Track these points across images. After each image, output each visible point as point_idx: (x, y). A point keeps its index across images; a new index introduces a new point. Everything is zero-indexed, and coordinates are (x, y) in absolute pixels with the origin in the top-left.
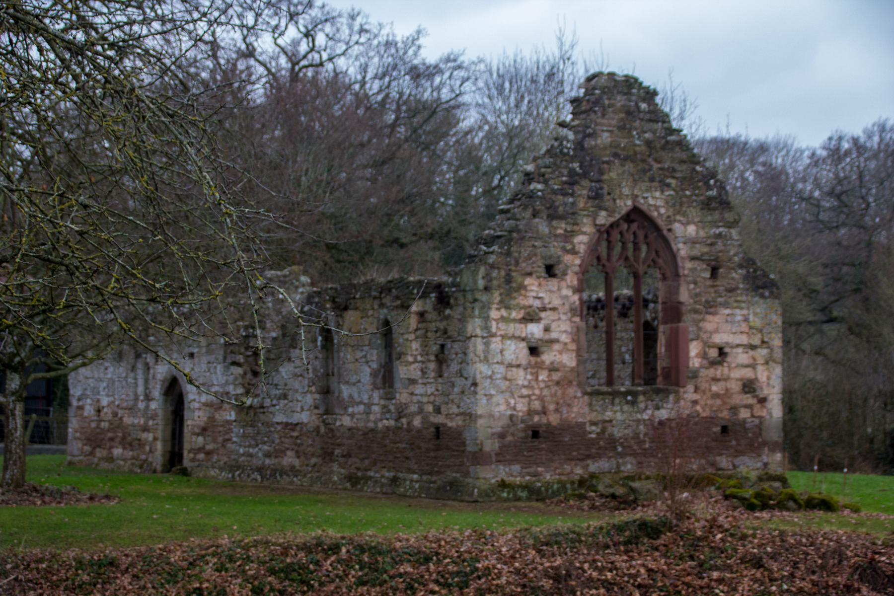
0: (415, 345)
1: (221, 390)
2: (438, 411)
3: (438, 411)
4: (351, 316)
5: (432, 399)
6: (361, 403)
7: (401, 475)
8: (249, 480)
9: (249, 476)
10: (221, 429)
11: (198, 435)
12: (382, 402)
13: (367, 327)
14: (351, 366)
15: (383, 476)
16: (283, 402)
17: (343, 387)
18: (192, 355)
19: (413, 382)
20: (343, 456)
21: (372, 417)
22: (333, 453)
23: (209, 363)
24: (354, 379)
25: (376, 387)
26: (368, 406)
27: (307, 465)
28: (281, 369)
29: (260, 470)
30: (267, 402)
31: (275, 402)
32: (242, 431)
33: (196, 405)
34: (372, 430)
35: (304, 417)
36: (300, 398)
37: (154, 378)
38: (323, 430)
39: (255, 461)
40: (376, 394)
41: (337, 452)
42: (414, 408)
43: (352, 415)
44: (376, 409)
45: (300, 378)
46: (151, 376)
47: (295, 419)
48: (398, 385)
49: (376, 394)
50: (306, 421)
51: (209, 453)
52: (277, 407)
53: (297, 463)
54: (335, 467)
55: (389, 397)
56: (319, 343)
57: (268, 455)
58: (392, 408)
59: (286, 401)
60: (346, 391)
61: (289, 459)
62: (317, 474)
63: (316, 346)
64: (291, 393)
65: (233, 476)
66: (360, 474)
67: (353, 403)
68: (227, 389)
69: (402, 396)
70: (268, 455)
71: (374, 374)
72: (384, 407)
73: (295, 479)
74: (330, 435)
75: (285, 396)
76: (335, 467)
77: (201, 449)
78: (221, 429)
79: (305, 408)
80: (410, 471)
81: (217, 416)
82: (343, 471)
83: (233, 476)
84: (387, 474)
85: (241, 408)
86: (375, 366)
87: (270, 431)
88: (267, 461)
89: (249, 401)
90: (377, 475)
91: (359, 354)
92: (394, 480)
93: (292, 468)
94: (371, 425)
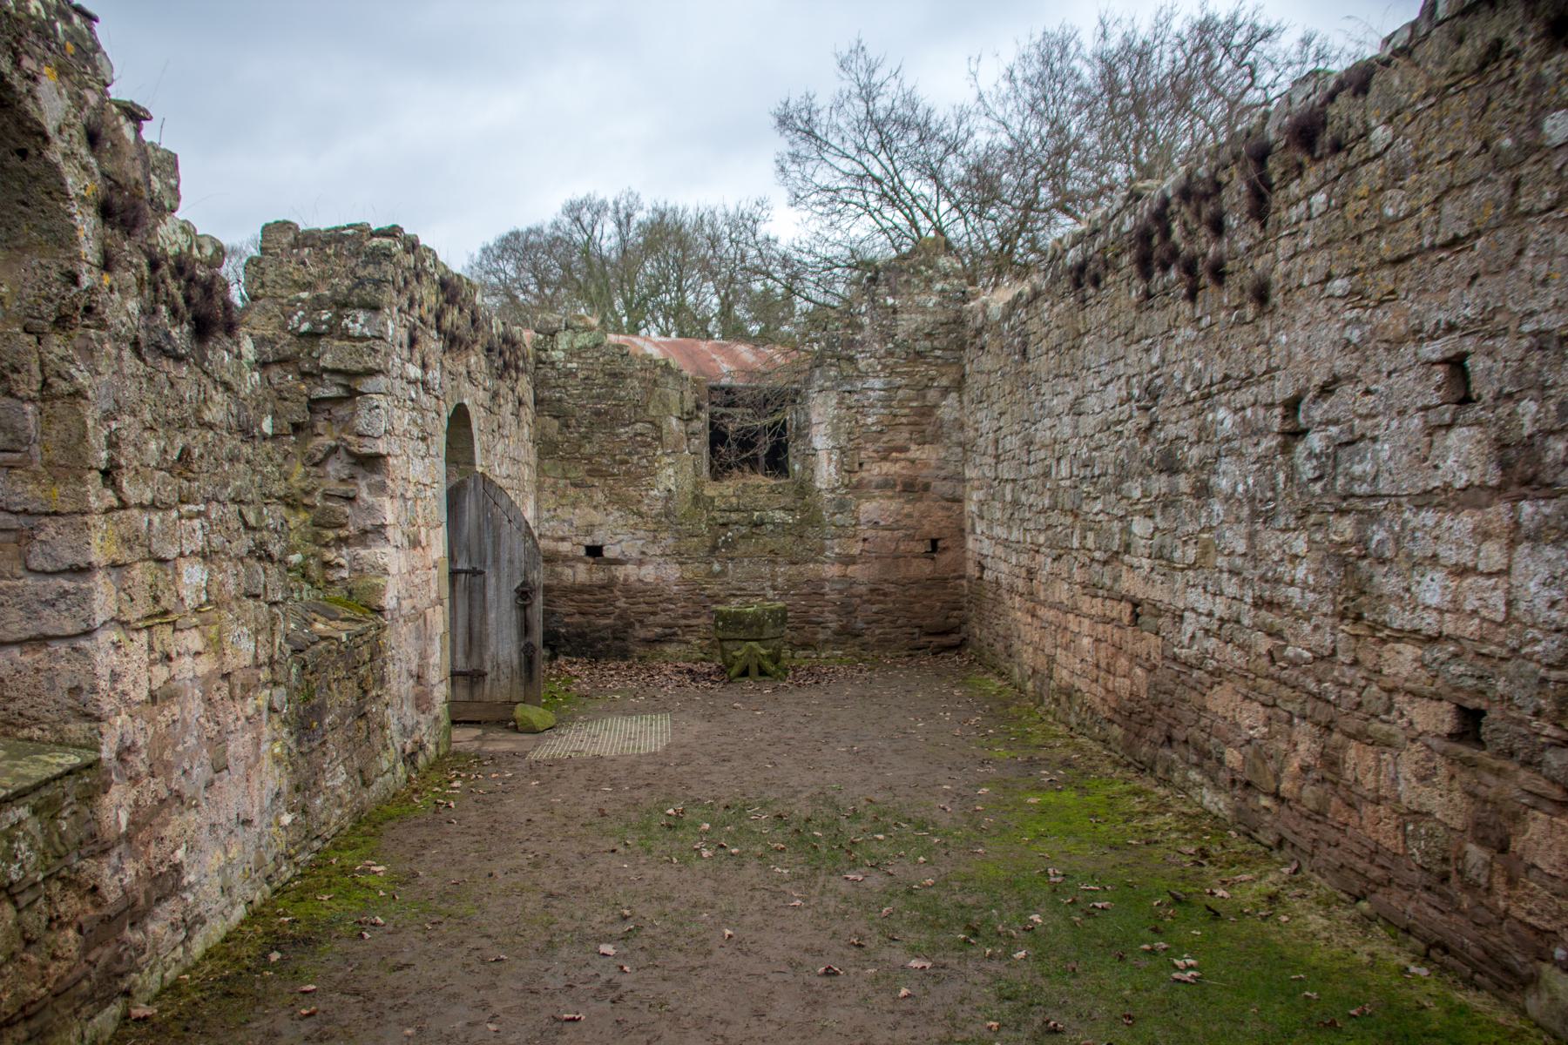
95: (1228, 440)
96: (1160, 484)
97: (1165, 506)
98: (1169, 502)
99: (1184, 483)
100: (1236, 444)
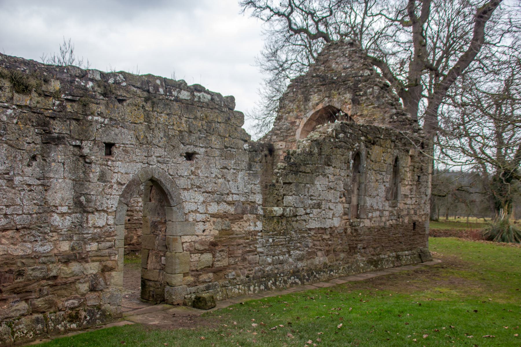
0: (409, 175)
1: (243, 199)
2: (415, 214)
3: (415, 214)
4: (376, 150)
5: (414, 206)
6: (378, 210)
7: (400, 253)
8: (288, 286)
9: (285, 282)
10: (241, 241)
11: (202, 252)
12: (390, 209)
13: (387, 159)
14: (372, 184)
15: (389, 256)
16: (315, 211)
17: (367, 199)
18: (189, 156)
19: (406, 196)
20: (364, 248)
21: (384, 219)
22: (356, 247)
23: (225, 168)
24: (375, 193)
25: (387, 199)
26: (382, 211)
27: (337, 260)
28: (316, 182)
29: (296, 273)
30: (301, 211)
31: (308, 211)
32: (271, 240)
33: (199, 217)
34: (383, 228)
35: (336, 222)
36: (332, 207)
37: (102, 178)
38: (349, 231)
39: (286, 267)
40: (387, 204)
41: (359, 246)
42: (405, 212)
43: (371, 219)
44: (387, 213)
45: (333, 191)
46: (94, 176)
47: (328, 224)
48: (399, 198)
49: (387, 204)
50: (337, 225)
51: (217, 271)
52: (311, 215)
53: (325, 259)
54: (358, 257)
55: (394, 206)
56: (351, 165)
57: (300, 259)
58: (395, 212)
59: (319, 210)
60: (369, 202)
61: (320, 259)
62: (347, 265)
63: (348, 168)
64: (323, 202)
65: (266, 287)
66: (375, 258)
67: (372, 209)
68: (251, 198)
69: (401, 205)
70: (300, 259)
71: (387, 191)
72: (391, 212)
73: (332, 273)
74: (355, 234)
75: (319, 206)
76: (358, 257)
77: (209, 268)
78: (241, 241)
79: (337, 215)
80: (403, 250)
81: (235, 228)
82: (364, 258)
83: (266, 287)
84: (391, 255)
85: (268, 218)
86: (388, 185)
87: (304, 237)
88: (300, 265)
89: (278, 210)
90: (386, 256)
91: (379, 177)
92: (398, 257)
93: (325, 264)
94: (382, 224)
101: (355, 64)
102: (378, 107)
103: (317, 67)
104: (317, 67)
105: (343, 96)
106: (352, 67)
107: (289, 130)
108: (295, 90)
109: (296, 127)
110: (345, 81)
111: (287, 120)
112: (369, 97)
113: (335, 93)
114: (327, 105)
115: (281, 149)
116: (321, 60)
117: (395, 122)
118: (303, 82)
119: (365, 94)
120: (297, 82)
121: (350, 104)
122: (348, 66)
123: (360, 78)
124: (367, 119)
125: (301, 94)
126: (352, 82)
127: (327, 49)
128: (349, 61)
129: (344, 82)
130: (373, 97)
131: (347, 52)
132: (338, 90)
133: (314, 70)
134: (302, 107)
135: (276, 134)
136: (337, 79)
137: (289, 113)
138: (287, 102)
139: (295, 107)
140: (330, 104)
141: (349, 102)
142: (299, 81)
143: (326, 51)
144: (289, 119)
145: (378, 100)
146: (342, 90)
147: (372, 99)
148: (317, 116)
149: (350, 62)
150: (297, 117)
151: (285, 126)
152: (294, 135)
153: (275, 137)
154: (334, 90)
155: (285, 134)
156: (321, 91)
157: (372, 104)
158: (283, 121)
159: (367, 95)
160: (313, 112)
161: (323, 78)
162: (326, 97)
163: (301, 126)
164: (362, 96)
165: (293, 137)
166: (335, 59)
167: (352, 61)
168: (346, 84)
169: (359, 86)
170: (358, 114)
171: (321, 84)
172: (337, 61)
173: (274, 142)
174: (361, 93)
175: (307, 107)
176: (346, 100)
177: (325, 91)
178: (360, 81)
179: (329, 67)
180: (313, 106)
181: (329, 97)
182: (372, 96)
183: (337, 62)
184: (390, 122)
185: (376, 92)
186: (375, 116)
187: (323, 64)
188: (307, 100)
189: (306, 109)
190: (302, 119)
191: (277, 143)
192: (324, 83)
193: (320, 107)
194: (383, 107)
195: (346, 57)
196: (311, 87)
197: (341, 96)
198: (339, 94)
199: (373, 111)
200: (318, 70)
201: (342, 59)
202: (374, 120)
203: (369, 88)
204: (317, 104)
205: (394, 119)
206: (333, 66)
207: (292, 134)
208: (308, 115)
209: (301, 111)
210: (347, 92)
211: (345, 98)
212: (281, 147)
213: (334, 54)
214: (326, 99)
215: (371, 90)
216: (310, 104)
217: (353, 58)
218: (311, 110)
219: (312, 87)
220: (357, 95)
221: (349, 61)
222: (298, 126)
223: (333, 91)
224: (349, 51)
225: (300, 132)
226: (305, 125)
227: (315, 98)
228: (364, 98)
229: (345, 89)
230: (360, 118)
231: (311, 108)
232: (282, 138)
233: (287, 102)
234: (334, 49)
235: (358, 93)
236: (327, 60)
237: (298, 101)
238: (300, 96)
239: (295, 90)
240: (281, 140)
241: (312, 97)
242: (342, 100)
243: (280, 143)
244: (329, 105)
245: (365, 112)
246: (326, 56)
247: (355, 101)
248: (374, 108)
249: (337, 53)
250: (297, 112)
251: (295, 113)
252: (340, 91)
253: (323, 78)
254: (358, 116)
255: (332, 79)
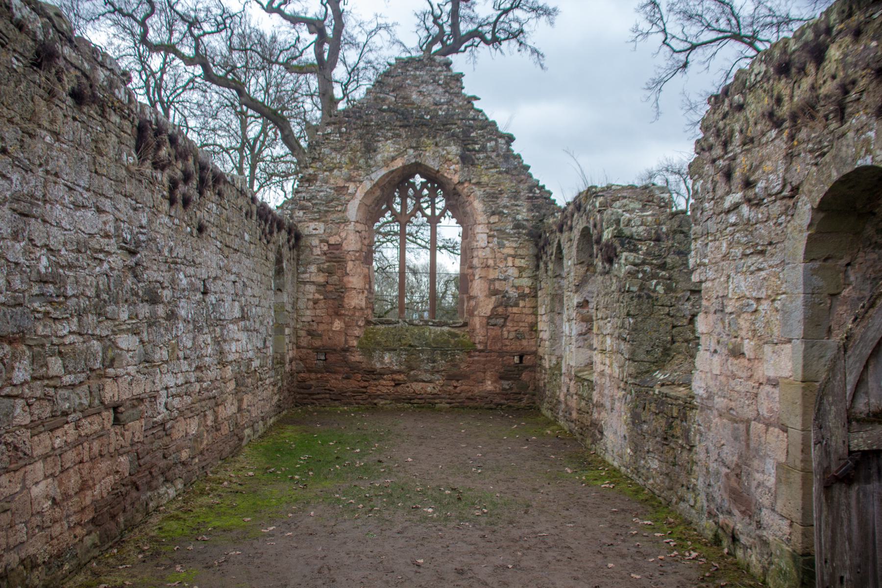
95: (184, 290)
96: (144, 310)
97: (150, 326)
98: (152, 323)
99: (161, 310)
100: (186, 293)
101: (456, 100)
102: (507, 172)
103: (382, 96)
104: (382, 96)
105: (443, 150)
106: (449, 103)
107: (332, 201)
108: (344, 130)
109: (347, 198)
110: (446, 123)
111: (327, 183)
112: (489, 154)
113: (428, 142)
114: (413, 161)
115: (315, 235)
116: (389, 85)
117: (537, 198)
118: (361, 117)
119: (483, 149)
120: (348, 116)
121: (457, 163)
122: (442, 101)
123: (471, 122)
124: (488, 189)
125: (357, 139)
126: (459, 128)
127: (402, 68)
128: (446, 92)
129: (444, 125)
130: (498, 155)
131: (442, 77)
132: (434, 137)
133: (375, 99)
134: (362, 161)
135: (302, 208)
136: (431, 118)
137: (331, 170)
138: (326, 150)
139: (345, 159)
140: (419, 160)
141: (454, 160)
142: (351, 115)
143: (399, 71)
144: (332, 181)
145: (506, 161)
146: (441, 139)
147: (496, 159)
148: (387, 180)
149: (447, 94)
150: (350, 179)
151: (322, 194)
152: (345, 210)
153: (301, 213)
154: (428, 137)
155: (323, 208)
156: (399, 136)
157: (495, 167)
158: (318, 183)
159: (486, 152)
160: (384, 171)
161: (403, 114)
162: (411, 147)
163: (360, 195)
164: (479, 152)
165: (341, 215)
166: (418, 87)
167: (450, 94)
168: (449, 130)
169: (472, 135)
170: (473, 181)
171: (401, 124)
172: (421, 88)
173: (300, 222)
174: (477, 147)
175: (372, 162)
176: (450, 157)
177: (407, 137)
178: (472, 127)
179: (404, 98)
180: (384, 161)
181: (415, 149)
182: (495, 154)
183: (420, 92)
184: (529, 198)
185: (502, 148)
186: (502, 187)
187: (393, 91)
188: (370, 149)
189: (370, 166)
190: (361, 182)
191: (306, 224)
192: (406, 122)
193: (399, 163)
194: (514, 172)
195: (439, 85)
196: (380, 127)
197: (440, 149)
198: (436, 145)
199: (498, 178)
200: (384, 100)
201: (430, 88)
202: (501, 192)
203: (490, 140)
204: (393, 159)
205: (535, 193)
206: (414, 96)
207: (339, 209)
208: (373, 176)
209: (357, 168)
210: (452, 143)
211: (448, 153)
212: (314, 232)
213: (415, 77)
214: (411, 151)
215: (493, 143)
216: (379, 157)
217: (451, 88)
218: (381, 168)
219: (382, 128)
220: (469, 150)
221: (446, 92)
222: (353, 195)
223: (423, 139)
224: (446, 77)
225: (357, 206)
226: (366, 194)
227: (387, 148)
228: (481, 156)
229: (447, 138)
230: (476, 188)
231: (381, 164)
232: (317, 216)
233: (326, 150)
234: (416, 69)
235: (470, 147)
236: (401, 86)
237: (351, 150)
238: (354, 142)
239: (344, 130)
240: (315, 220)
241: (380, 145)
242: (443, 156)
243: (312, 225)
244: (416, 162)
245: (485, 179)
246: (399, 79)
247: (466, 160)
248: (500, 173)
249: (422, 76)
250: (349, 170)
251: (345, 171)
252: (438, 139)
253: (403, 114)
254: (474, 184)
255: (422, 117)
